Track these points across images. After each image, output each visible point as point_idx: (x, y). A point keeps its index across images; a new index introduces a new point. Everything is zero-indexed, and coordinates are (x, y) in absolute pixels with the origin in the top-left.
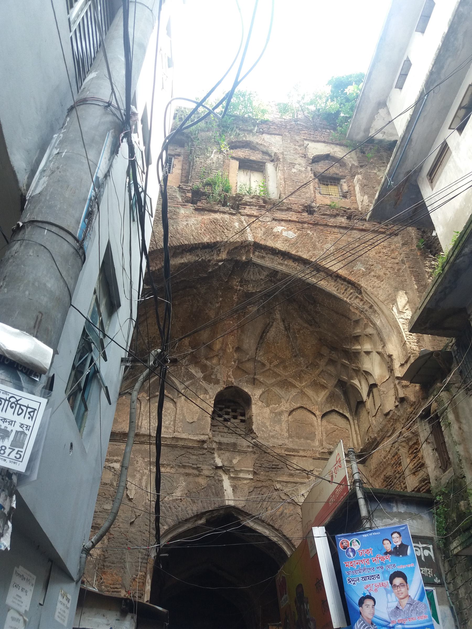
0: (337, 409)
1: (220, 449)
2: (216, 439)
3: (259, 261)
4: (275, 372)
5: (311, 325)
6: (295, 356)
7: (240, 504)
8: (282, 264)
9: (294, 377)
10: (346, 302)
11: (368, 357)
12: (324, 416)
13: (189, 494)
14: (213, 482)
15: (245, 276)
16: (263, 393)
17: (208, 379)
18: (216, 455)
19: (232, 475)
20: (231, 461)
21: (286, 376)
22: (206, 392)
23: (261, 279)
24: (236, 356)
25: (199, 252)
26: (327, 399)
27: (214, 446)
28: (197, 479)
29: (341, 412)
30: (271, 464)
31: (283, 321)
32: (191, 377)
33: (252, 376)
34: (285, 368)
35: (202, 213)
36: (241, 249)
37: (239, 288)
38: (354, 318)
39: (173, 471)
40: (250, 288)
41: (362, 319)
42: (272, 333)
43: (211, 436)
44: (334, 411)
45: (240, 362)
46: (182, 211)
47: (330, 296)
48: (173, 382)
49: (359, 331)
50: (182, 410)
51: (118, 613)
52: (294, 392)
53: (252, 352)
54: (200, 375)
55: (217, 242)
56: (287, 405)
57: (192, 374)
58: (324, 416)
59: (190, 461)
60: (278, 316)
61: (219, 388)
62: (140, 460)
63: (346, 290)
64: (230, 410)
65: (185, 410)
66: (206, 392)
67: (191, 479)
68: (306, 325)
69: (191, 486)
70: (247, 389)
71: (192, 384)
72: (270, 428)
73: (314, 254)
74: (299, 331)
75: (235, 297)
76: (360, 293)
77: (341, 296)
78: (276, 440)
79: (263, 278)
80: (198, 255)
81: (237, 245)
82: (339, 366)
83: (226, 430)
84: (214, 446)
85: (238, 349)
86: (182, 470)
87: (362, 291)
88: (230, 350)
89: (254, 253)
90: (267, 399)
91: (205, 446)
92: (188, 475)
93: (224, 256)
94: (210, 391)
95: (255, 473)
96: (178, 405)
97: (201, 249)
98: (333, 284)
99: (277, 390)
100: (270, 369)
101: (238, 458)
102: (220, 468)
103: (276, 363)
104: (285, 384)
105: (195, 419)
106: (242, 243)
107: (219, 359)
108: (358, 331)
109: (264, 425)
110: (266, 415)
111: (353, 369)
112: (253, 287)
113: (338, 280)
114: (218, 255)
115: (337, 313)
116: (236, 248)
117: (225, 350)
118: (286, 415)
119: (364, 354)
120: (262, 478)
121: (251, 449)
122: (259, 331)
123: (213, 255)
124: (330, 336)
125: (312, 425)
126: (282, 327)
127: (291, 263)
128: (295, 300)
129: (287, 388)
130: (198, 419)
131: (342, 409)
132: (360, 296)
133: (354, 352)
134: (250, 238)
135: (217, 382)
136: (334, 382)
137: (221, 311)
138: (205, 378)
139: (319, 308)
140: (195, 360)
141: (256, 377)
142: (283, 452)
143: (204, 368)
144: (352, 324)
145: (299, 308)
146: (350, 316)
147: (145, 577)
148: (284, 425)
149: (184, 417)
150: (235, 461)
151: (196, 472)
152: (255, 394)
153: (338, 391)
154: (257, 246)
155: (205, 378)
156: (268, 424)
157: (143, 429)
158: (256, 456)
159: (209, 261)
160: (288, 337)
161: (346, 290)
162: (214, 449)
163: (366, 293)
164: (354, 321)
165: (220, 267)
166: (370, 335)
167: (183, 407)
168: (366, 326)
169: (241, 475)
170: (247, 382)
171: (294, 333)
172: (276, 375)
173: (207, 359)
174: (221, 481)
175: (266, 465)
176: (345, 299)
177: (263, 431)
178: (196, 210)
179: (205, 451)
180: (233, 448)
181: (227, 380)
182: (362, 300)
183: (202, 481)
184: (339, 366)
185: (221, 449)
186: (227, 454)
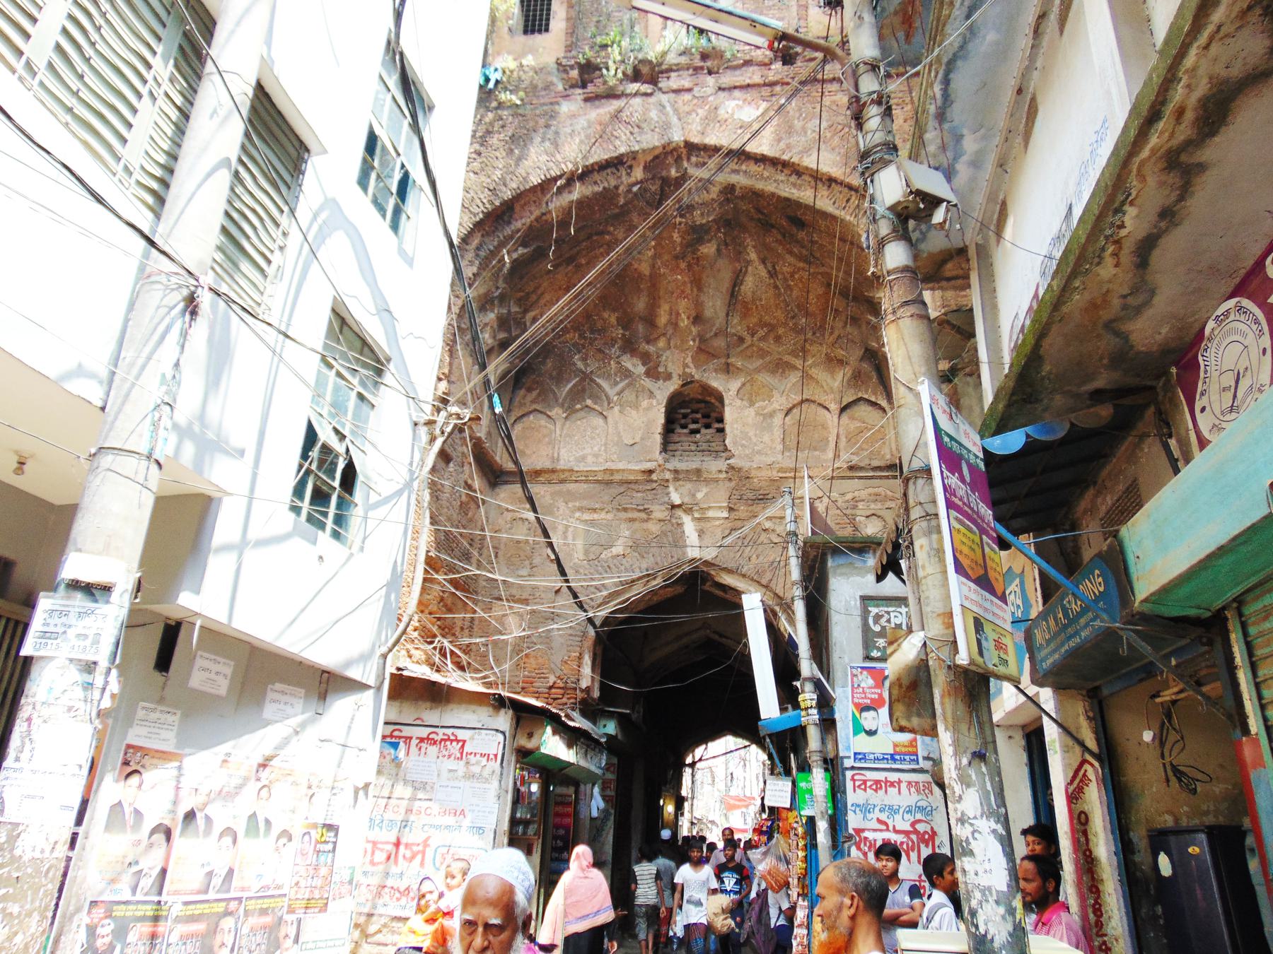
0: (866, 396)
1: (676, 479)
2: (670, 466)
4: (761, 349)
5: (810, 263)
6: (793, 318)
7: (709, 554)
9: (794, 353)
12: (843, 410)
13: (635, 546)
14: (669, 527)
16: (744, 385)
17: (653, 373)
18: (671, 489)
19: (697, 515)
20: (694, 495)
21: (779, 353)
22: (651, 394)
24: (694, 330)
25: (596, 176)
26: (849, 381)
27: (668, 475)
28: (645, 525)
29: (873, 399)
30: (751, 494)
31: (763, 261)
32: (627, 374)
33: (723, 360)
34: (778, 339)
35: (597, 103)
36: (666, 158)
37: (678, 219)
39: (610, 516)
40: (699, 218)
42: (749, 284)
43: (661, 462)
44: (860, 399)
45: (702, 339)
46: (565, 108)
48: (599, 386)
50: (617, 428)
51: (491, 709)
52: (794, 377)
53: (719, 322)
54: (641, 369)
55: (622, 155)
56: (783, 400)
57: (627, 370)
58: (843, 410)
59: (634, 501)
60: (753, 256)
61: (673, 386)
62: (562, 505)
64: (699, 416)
65: (621, 427)
66: (651, 394)
67: (637, 525)
68: (802, 265)
69: (638, 536)
70: (716, 383)
71: (628, 385)
72: (754, 440)
73: (789, 147)
74: (792, 276)
75: (676, 235)
78: (763, 458)
79: (715, 196)
80: (596, 183)
81: (657, 152)
82: (864, 327)
83: (693, 448)
84: (668, 475)
85: (697, 319)
86: (623, 515)
88: (684, 322)
89: (689, 159)
90: (750, 395)
91: (654, 477)
92: (632, 520)
93: (638, 174)
94: (657, 393)
95: (731, 509)
96: (610, 419)
97: (598, 172)
99: (765, 378)
100: (752, 345)
101: (705, 490)
102: (679, 506)
103: (761, 333)
104: (780, 367)
105: (637, 440)
106: (664, 148)
107: (669, 340)
109: (745, 436)
110: (750, 421)
112: (702, 214)
114: (629, 174)
116: (656, 157)
117: (676, 324)
118: (780, 416)
120: (743, 515)
121: (723, 475)
122: (726, 285)
123: (620, 177)
125: (824, 427)
126: (764, 273)
127: (753, 168)
128: (773, 226)
129: (784, 372)
130: (642, 439)
131: (875, 394)
134: (677, 137)
135: (668, 377)
136: (859, 353)
137: (659, 262)
138: (648, 374)
140: (629, 347)
141: (729, 361)
142: (776, 475)
143: (645, 358)
145: (784, 236)
147: (580, 658)
148: (778, 434)
149: (620, 437)
150: (700, 495)
151: (643, 515)
152: (729, 388)
153: (866, 366)
154: (691, 147)
155: (648, 374)
156: (751, 434)
157: (562, 462)
158: (733, 484)
159: (616, 187)
160: (776, 287)
161: (848, 201)
162: (667, 481)
165: (636, 194)
167: (616, 423)
169: (711, 514)
170: (716, 371)
171: (785, 279)
172: (763, 353)
173: (648, 342)
174: (680, 525)
175: (750, 495)
176: (848, 218)
177: (743, 446)
178: (586, 100)
179: (654, 485)
180: (697, 475)
181: (684, 373)
183: (654, 527)
184: (864, 327)
185: (679, 480)
186: (689, 485)
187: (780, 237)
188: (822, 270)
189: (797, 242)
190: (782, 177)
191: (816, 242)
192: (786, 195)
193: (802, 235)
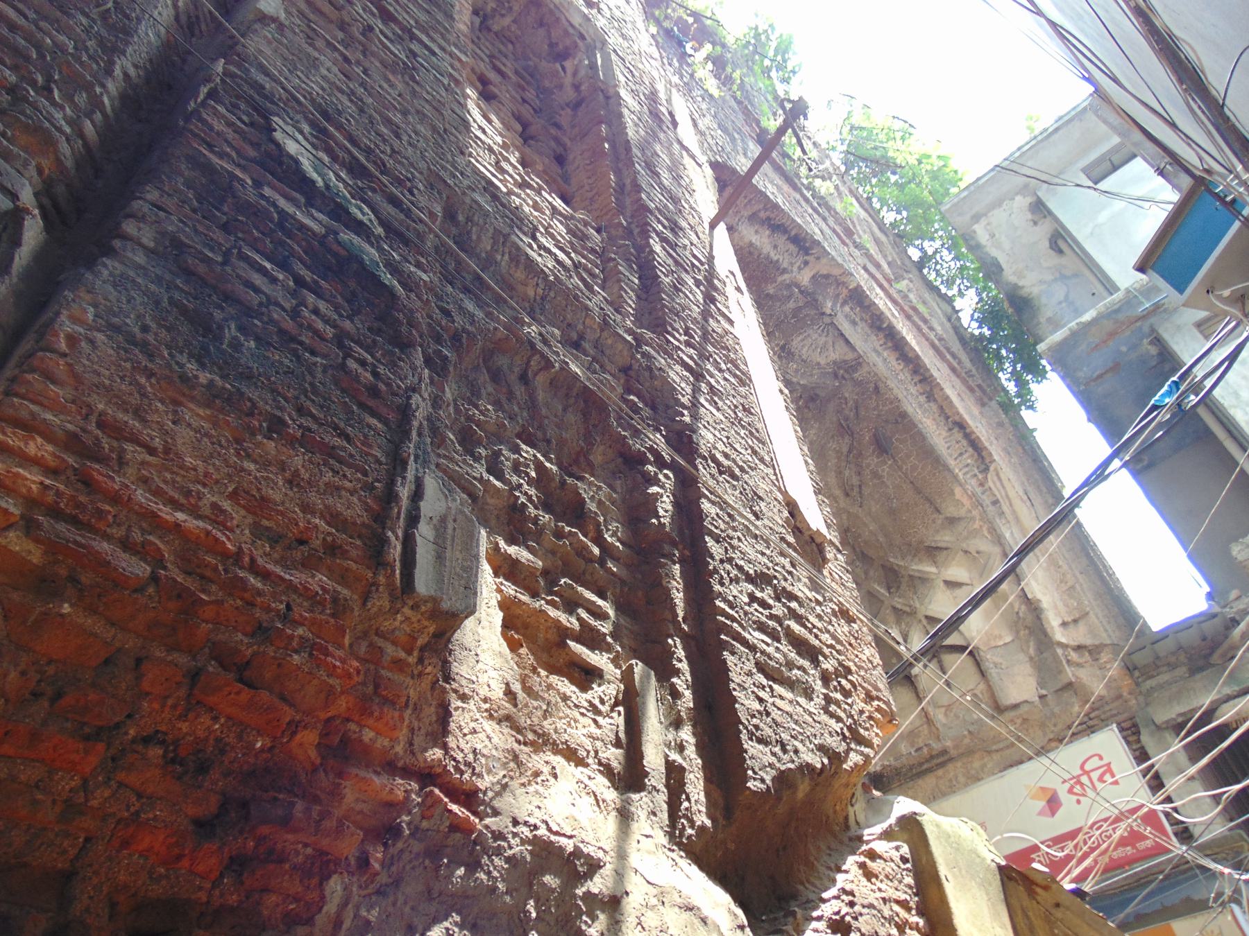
3: (846, 327)
5: (847, 495)
8: (879, 354)
10: (955, 477)
11: (948, 592)
15: (796, 343)
23: (818, 364)
38: (951, 511)
41: (973, 519)
47: (929, 454)
49: (947, 538)
63: (961, 454)
76: (986, 470)
77: (951, 463)
79: (823, 362)
80: (775, 247)
87: (992, 468)
93: (805, 278)
98: (944, 434)
108: (945, 538)
111: (894, 608)
112: (797, 371)
113: (956, 430)
115: (918, 491)
119: (942, 584)
124: (871, 532)
132: (980, 476)
133: (911, 576)
139: (885, 470)
144: (939, 522)
145: (850, 452)
146: (944, 506)
159: (784, 271)
161: (961, 454)
163: (998, 475)
164: (947, 518)
166: (978, 552)
168: (975, 533)
182: (982, 485)
187: (845, 450)
188: (855, 509)
189: (858, 465)
190: (913, 390)
191: (880, 477)
192: (910, 410)
193: (872, 461)
